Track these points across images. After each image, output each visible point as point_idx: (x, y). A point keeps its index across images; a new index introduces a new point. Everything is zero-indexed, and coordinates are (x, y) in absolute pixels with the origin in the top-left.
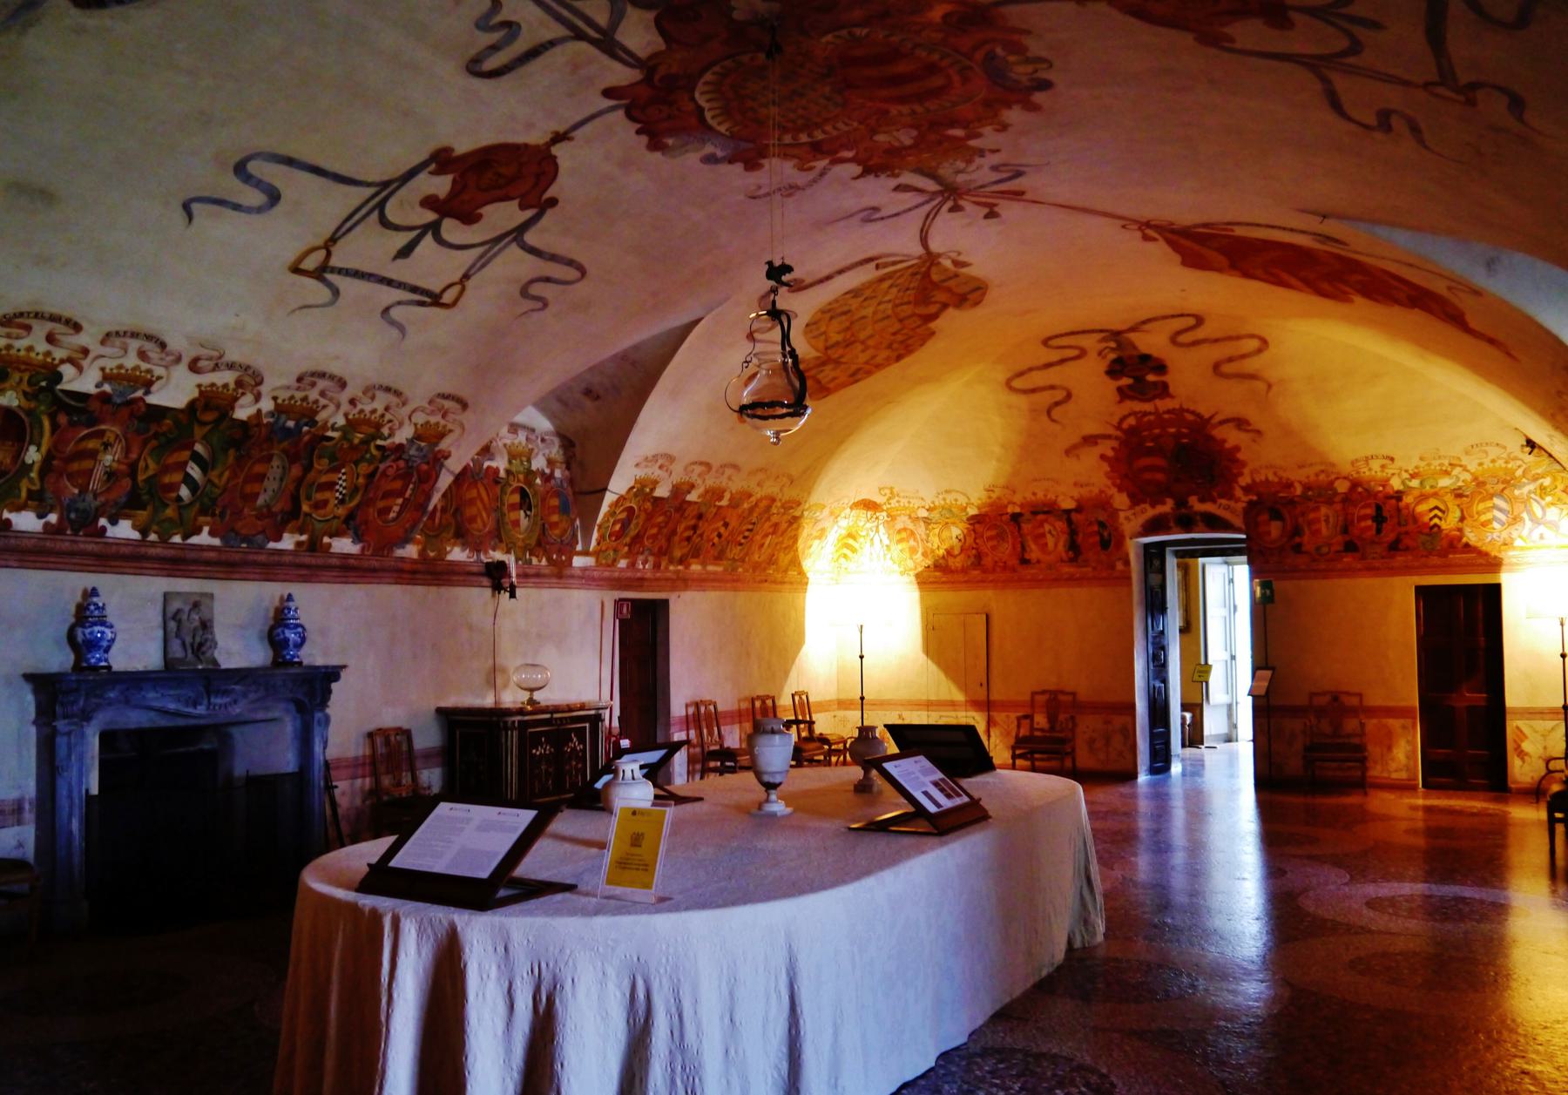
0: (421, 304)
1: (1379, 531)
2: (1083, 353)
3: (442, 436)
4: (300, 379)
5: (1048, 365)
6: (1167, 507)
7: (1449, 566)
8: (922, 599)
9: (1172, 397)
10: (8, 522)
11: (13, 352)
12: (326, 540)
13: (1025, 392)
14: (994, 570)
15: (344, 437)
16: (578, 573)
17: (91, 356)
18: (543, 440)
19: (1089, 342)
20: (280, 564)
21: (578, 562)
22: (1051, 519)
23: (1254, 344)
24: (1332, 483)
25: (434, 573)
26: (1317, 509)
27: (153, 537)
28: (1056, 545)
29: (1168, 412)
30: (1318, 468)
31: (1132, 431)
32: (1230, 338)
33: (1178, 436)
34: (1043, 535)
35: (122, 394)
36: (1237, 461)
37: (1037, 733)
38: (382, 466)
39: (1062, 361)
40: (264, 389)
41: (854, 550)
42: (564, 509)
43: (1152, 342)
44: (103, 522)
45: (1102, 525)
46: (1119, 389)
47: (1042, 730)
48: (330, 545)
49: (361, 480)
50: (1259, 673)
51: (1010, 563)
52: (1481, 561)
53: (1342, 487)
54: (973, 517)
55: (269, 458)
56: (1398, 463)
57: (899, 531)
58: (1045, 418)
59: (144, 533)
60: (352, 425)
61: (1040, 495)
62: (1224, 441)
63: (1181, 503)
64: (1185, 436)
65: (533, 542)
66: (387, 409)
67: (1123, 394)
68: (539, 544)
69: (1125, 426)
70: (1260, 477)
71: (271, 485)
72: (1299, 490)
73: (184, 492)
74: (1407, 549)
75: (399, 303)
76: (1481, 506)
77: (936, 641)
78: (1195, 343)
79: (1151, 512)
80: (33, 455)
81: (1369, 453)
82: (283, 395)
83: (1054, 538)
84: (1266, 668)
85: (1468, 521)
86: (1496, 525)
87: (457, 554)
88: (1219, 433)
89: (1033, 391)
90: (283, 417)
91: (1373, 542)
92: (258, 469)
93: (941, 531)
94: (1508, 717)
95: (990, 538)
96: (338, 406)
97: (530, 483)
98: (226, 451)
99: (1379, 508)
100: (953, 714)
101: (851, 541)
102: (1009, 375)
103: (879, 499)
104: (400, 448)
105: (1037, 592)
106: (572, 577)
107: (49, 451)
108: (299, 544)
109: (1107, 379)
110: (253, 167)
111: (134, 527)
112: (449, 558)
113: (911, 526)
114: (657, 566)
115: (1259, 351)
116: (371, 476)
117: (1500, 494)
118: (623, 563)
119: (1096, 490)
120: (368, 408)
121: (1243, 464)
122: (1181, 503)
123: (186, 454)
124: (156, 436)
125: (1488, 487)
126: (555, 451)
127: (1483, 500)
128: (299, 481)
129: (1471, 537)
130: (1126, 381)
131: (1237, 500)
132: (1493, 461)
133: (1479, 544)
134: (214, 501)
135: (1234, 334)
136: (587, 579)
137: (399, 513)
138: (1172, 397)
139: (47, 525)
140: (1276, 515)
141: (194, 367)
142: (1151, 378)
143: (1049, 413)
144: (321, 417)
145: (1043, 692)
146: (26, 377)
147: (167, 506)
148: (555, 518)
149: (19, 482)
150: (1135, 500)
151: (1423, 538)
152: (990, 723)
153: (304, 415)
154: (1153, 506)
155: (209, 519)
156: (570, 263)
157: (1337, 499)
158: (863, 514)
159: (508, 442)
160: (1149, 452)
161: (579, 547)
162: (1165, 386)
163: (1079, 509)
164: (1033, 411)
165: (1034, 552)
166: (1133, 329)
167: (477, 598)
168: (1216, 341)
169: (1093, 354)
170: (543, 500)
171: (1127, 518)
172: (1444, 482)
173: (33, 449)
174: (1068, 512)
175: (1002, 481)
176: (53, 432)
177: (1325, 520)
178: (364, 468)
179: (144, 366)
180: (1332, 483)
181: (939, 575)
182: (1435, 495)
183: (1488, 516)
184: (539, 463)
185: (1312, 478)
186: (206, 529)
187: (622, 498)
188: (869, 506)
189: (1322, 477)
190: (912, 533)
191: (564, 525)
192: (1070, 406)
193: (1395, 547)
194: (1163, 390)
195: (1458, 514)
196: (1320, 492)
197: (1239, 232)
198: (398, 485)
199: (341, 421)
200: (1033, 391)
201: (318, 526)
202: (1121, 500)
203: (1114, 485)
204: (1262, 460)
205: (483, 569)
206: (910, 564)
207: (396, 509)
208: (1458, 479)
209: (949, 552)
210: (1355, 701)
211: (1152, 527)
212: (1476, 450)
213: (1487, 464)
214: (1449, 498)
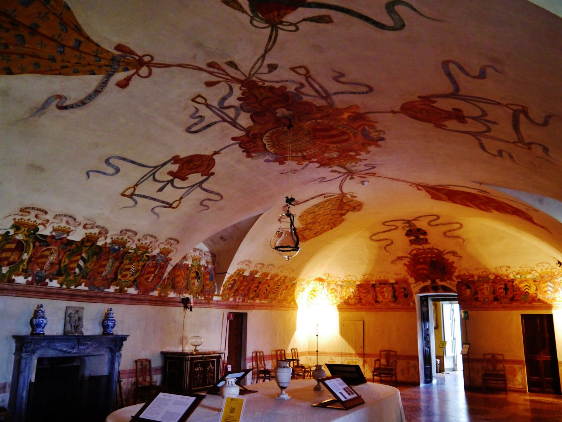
0: (165, 207)
1: (506, 293)
2: (397, 228)
3: (169, 252)
4: (121, 232)
6: (428, 283)
7: (533, 307)
8: (339, 314)
9: (429, 244)
10: (14, 280)
11: (23, 221)
12: (126, 289)
13: (376, 241)
14: (365, 305)
15: (135, 252)
16: (215, 302)
17: (50, 223)
18: (205, 254)
19: (399, 224)
20: (108, 297)
21: (215, 298)
22: (387, 286)
23: (458, 226)
24: (488, 275)
25: (163, 301)
26: (483, 285)
27: (64, 286)
28: (388, 296)
29: (428, 249)
30: (482, 270)
31: (415, 255)
32: (449, 224)
34: (383, 292)
35: (59, 236)
36: (454, 267)
37: (382, 367)
38: (147, 263)
39: (389, 230)
40: (108, 235)
41: (315, 296)
42: (211, 279)
43: (422, 224)
44: (47, 280)
45: (405, 289)
46: (410, 241)
47: (384, 365)
48: (127, 291)
49: (140, 268)
50: (464, 345)
52: (545, 305)
53: (492, 277)
54: (358, 285)
55: (108, 259)
56: (511, 269)
57: (331, 290)
59: (61, 285)
60: (138, 248)
61: (382, 278)
62: (448, 260)
63: (433, 282)
64: (434, 257)
65: (199, 291)
66: (151, 243)
67: (412, 242)
68: (202, 291)
69: (412, 253)
70: (462, 273)
71: (108, 269)
72: (476, 278)
73: (77, 271)
74: (517, 300)
75: (158, 207)
76: (543, 285)
77: (345, 331)
78: (437, 225)
79: (422, 285)
80: (26, 256)
81: (501, 265)
82: (115, 237)
83: (388, 293)
84: (467, 344)
85: (539, 291)
86: (549, 292)
87: (172, 295)
88: (446, 257)
89: (380, 240)
90: (114, 245)
91: (504, 298)
92: (104, 263)
94: (559, 365)
95: (364, 293)
96: (134, 241)
97: (199, 269)
98: (93, 256)
100: (350, 358)
101: (314, 293)
102: (371, 234)
103: (324, 278)
104: (154, 256)
106: (213, 304)
107: (31, 255)
108: (116, 290)
109: (405, 237)
110: (111, 161)
111: (58, 283)
112: (169, 296)
113: (335, 288)
114: (244, 300)
115: (460, 228)
116: (143, 266)
117: (550, 281)
118: (231, 299)
119: (402, 277)
120: (144, 242)
121: (455, 268)
122: (433, 282)
123: (79, 257)
124: (69, 250)
125: (545, 278)
126: (209, 258)
127: (544, 283)
128: (118, 268)
129: (540, 296)
131: (454, 281)
132: (546, 269)
133: (543, 299)
134: (87, 274)
136: (218, 305)
137: (152, 280)
138: (429, 244)
139: (27, 281)
140: (468, 287)
141: (85, 227)
142: (421, 237)
143: (385, 248)
144: (128, 245)
145: (384, 351)
146: (26, 229)
147: (70, 275)
148: (208, 282)
149: (19, 266)
150: (417, 280)
151: (522, 296)
152: (364, 362)
153: (121, 244)
154: (423, 282)
155: (84, 280)
156: (218, 194)
157: (490, 281)
158: (319, 283)
159: (193, 255)
160: (422, 263)
161: (216, 293)
162: (427, 240)
163: (397, 283)
164: (380, 248)
165: (380, 298)
166: (415, 220)
167: (178, 310)
168: (444, 224)
169: (400, 228)
170: (204, 276)
171: (414, 287)
172: (529, 276)
173: (26, 254)
174: (392, 284)
175: (368, 272)
176: (34, 248)
177: (487, 289)
178: (141, 263)
179: (68, 226)
180: (488, 275)
181: (345, 306)
182: (526, 281)
183: (546, 289)
184: (203, 262)
185: (481, 274)
186: (83, 284)
187: (232, 276)
188: (321, 280)
189: (484, 273)
190: (336, 290)
191: (211, 285)
192: (393, 246)
193: (512, 300)
194: (426, 241)
195: (535, 288)
196: (484, 278)
197: (451, 188)
198: (153, 269)
199: (134, 247)
200: (380, 240)
201: (124, 284)
202: (411, 280)
204: (462, 267)
205: (181, 300)
206: (335, 302)
207: (151, 278)
208: (534, 275)
209: (349, 298)
210: (501, 357)
211: (423, 290)
212: (540, 265)
214: (531, 282)
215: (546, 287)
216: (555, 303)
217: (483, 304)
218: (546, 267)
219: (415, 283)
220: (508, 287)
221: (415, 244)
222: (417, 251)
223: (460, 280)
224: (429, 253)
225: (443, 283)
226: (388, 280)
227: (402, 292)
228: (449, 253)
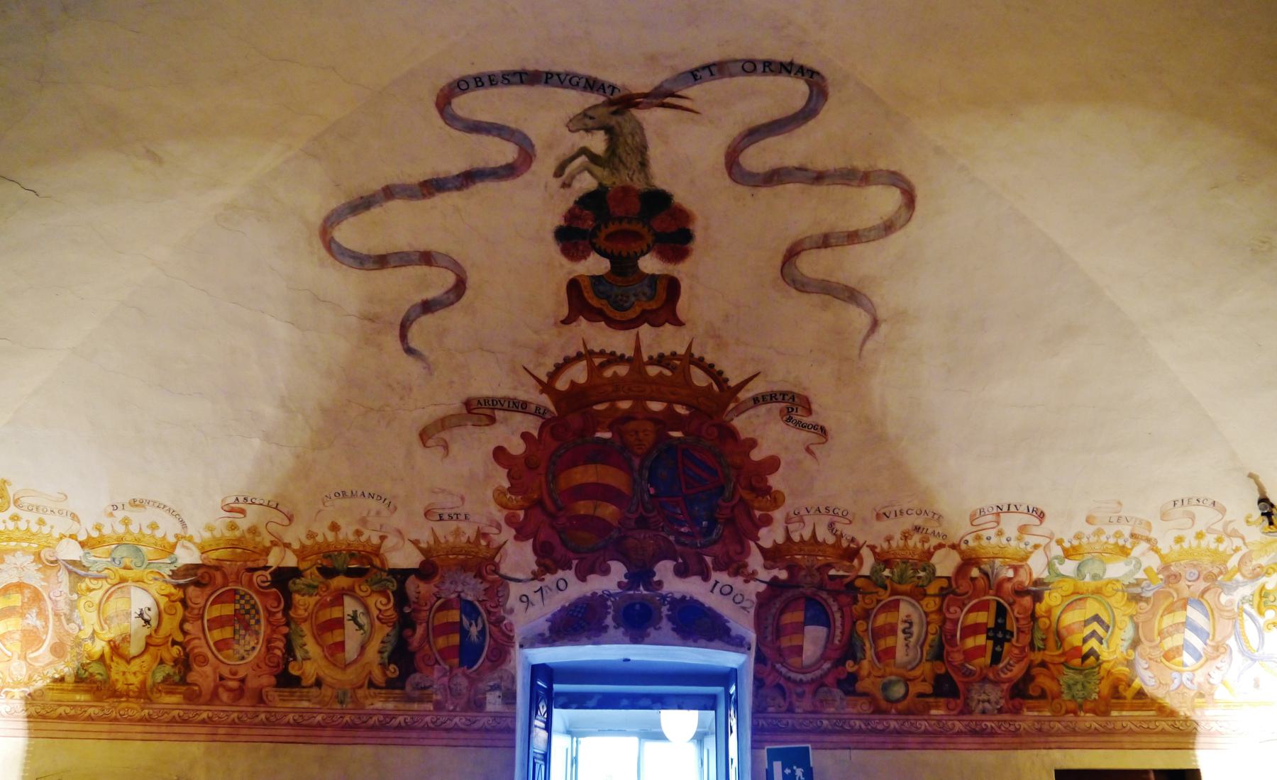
1: (996, 658)
5: (433, 187)
7: (1111, 732)
9: (678, 323)
22: (363, 589)
26: (894, 606)
28: (363, 648)
29: (661, 360)
30: (907, 522)
31: (575, 399)
34: (338, 624)
39: (469, 178)
43: (682, 154)
45: (469, 609)
46: (574, 286)
51: (252, 683)
52: (1163, 725)
53: (945, 564)
54: (190, 569)
58: (392, 341)
61: (347, 533)
62: (753, 443)
63: (641, 574)
64: (678, 422)
67: (580, 300)
69: (562, 384)
70: (801, 533)
74: (1043, 695)
76: (1168, 621)
78: (775, 177)
81: (1004, 502)
83: (363, 631)
85: (1145, 647)
86: (1187, 658)
88: (743, 424)
89: (382, 261)
91: (984, 679)
93: (108, 596)
95: (218, 622)
99: (1001, 612)
105: (308, 752)
109: (554, 249)
113: (34, 578)
119: (469, 531)
122: (641, 574)
125: (1183, 583)
127: (1170, 610)
129: (1147, 678)
130: (596, 265)
132: (1200, 536)
135: (861, 164)
138: (678, 323)
142: (650, 264)
150: (548, 561)
151: (1069, 676)
154: (582, 578)
157: (933, 589)
160: (602, 454)
162: (673, 286)
163: (426, 571)
165: (311, 660)
166: (661, 97)
168: (819, 178)
172: (1117, 570)
175: (265, 492)
177: (907, 626)
185: (897, 542)
189: (915, 540)
190: (37, 597)
192: (453, 318)
194: (664, 302)
195: (1128, 633)
196: (905, 572)
200: (382, 261)
202: (518, 557)
203: (510, 521)
204: (817, 495)
206: (19, 670)
209: (115, 648)
212: (1179, 510)
213: (1190, 541)
214: (1118, 601)
215: (1179, 627)
216: (1209, 712)
217: (878, 710)
218: (1200, 526)
219: (536, 576)
220: (1011, 625)
221: (594, 315)
222: (593, 371)
223: (783, 575)
224: (657, 388)
225: (692, 588)
226: (376, 551)
227: (447, 628)
228: (770, 397)
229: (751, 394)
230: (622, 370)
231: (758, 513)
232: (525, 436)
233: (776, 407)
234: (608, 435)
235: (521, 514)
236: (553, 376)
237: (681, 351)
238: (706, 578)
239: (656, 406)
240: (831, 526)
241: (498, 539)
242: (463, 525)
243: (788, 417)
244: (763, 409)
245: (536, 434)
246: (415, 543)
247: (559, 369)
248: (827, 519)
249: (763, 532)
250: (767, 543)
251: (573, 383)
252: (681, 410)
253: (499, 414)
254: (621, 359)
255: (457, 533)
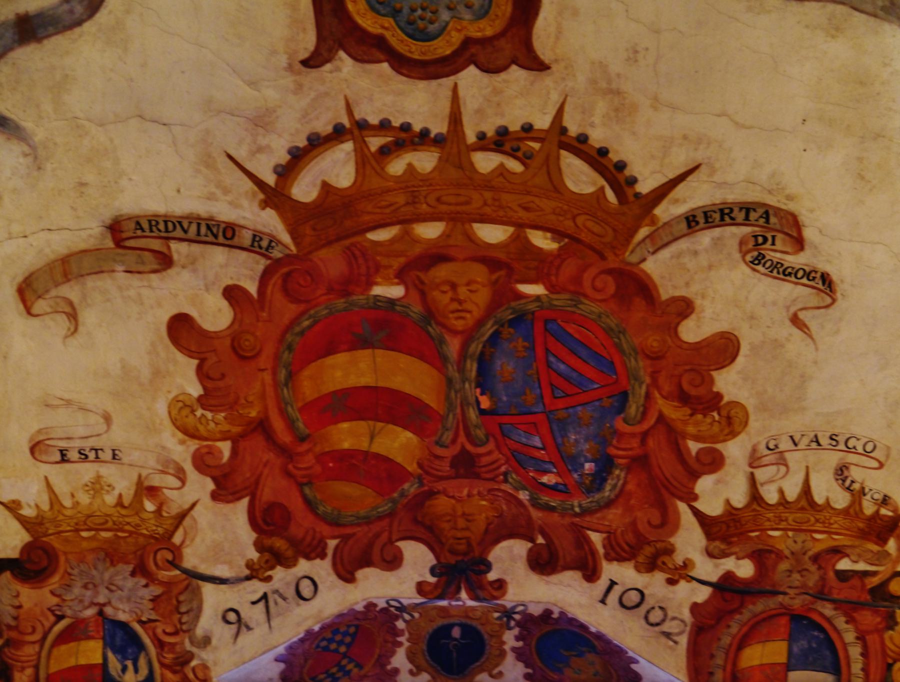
9: (537, 65)
29: (501, 141)
31: (334, 215)
33: (506, 265)
36: (714, 402)
45: (123, 640)
62: (684, 308)
63: (462, 568)
64: (541, 267)
69: (304, 190)
79: (334, 598)
88: (661, 268)
119: (121, 483)
121: (732, 420)
131: (680, 573)
138: (537, 65)
150: (279, 539)
154: (347, 575)
160: (387, 329)
171: (235, 620)
202: (219, 535)
203: (201, 462)
219: (255, 572)
221: (370, 48)
222: (363, 160)
223: (745, 569)
229: (681, 209)
230: (425, 161)
231: (694, 447)
232: (232, 294)
233: (733, 234)
234: (396, 291)
235: (225, 447)
236: (288, 171)
237: (543, 122)
238: (591, 575)
239: (492, 234)
240: (841, 472)
241: (178, 499)
242: (109, 472)
243: (756, 256)
244: (705, 238)
245: (252, 288)
246: (13, 507)
247: (298, 158)
248: (833, 459)
249: (704, 484)
250: (712, 507)
251: (326, 187)
252: (542, 241)
253: (179, 249)
254: (424, 139)
255: (97, 486)
